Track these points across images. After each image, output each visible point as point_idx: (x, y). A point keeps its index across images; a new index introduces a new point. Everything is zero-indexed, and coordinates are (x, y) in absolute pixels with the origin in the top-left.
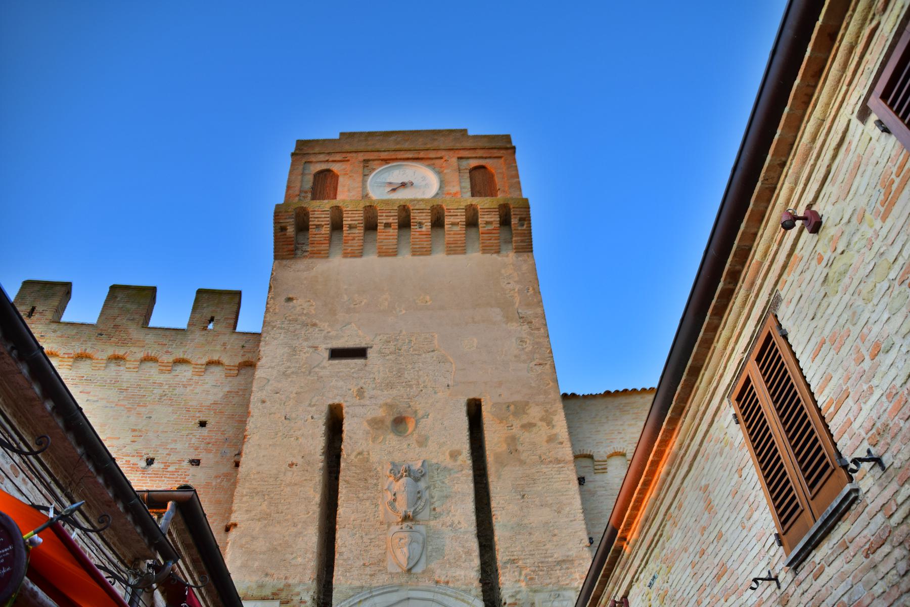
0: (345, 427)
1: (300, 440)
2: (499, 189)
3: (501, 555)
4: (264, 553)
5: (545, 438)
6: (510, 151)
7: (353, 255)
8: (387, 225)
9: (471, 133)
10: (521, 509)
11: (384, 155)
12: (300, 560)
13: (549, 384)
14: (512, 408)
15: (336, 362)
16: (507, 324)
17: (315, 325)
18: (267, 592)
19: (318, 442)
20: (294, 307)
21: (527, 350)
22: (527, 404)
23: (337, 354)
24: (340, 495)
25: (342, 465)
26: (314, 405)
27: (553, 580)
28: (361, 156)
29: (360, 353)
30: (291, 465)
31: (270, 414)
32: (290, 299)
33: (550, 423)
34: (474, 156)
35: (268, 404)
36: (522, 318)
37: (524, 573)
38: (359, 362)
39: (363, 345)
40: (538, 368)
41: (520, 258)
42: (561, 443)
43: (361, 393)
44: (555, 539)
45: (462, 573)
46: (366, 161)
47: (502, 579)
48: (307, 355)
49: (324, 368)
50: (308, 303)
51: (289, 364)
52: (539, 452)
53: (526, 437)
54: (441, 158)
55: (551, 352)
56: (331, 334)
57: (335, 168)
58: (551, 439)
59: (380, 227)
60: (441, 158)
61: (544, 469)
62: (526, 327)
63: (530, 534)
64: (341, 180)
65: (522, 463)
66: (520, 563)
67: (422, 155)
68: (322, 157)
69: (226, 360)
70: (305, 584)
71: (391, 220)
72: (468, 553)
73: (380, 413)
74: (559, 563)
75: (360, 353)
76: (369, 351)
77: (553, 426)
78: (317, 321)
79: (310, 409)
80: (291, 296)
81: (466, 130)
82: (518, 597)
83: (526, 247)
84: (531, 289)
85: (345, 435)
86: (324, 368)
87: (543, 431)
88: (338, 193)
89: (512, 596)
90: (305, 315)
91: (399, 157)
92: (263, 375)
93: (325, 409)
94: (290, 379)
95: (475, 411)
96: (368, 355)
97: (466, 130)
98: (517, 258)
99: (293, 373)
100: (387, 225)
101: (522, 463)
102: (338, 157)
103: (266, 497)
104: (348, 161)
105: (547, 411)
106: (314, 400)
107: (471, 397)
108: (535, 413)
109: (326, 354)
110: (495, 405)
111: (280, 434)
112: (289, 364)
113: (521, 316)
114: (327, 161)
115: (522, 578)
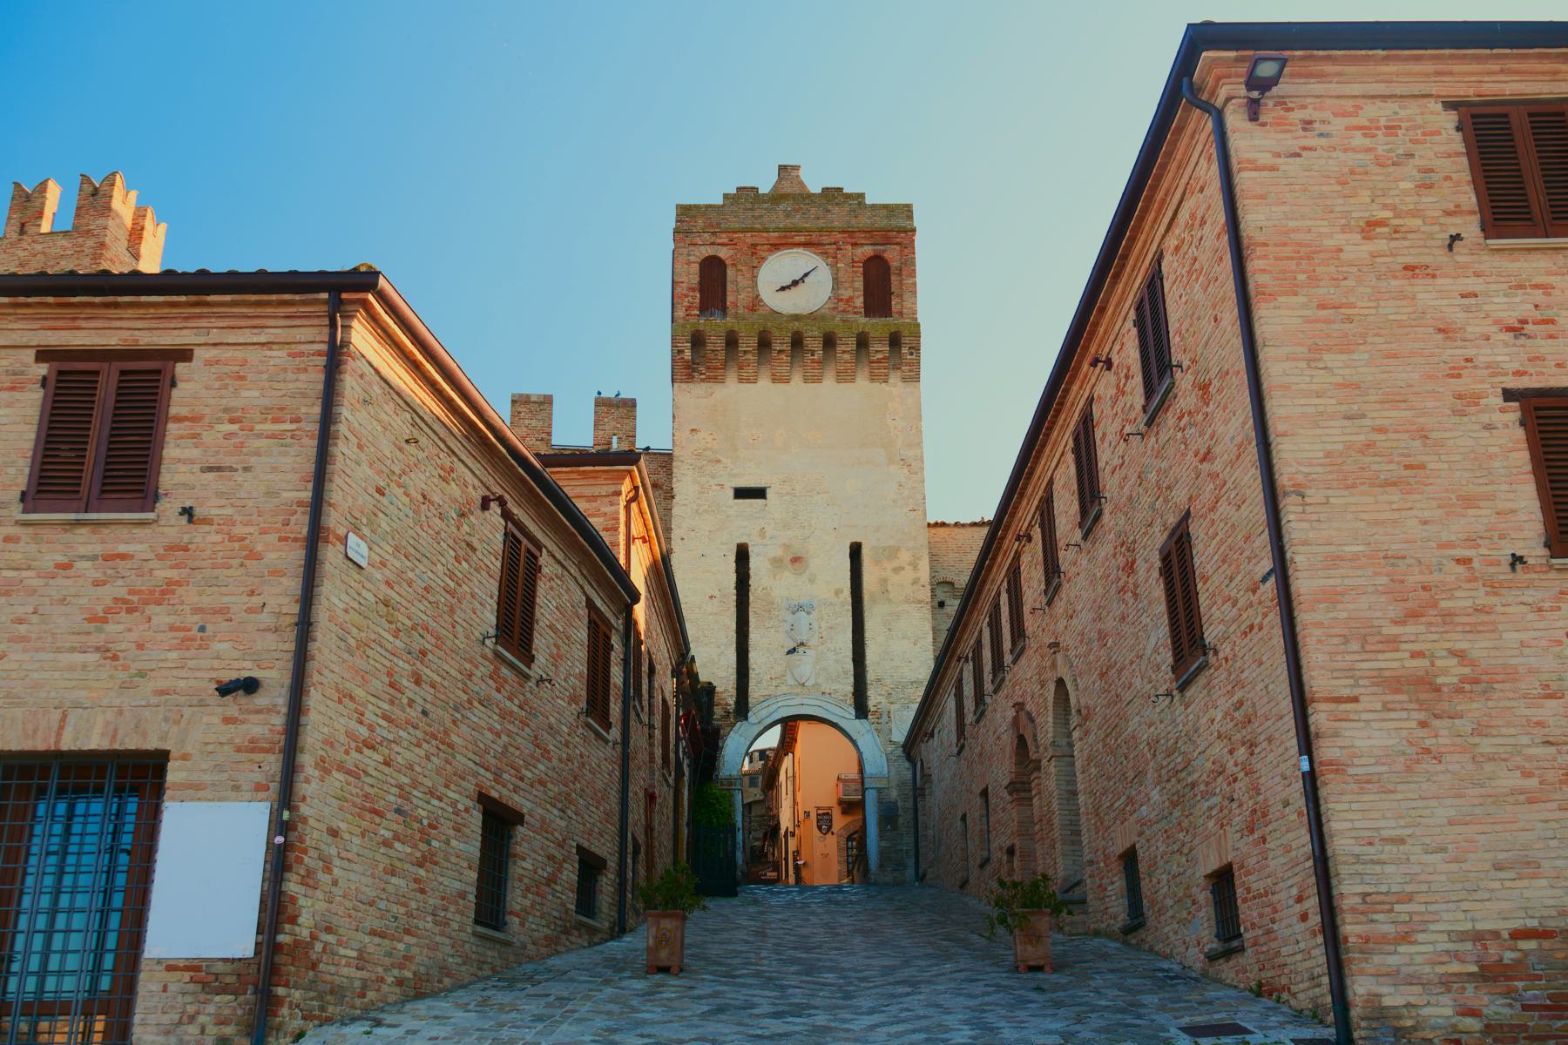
7: (748, 381)
8: (780, 352)
9: (869, 201)
17: (719, 461)
22: (898, 549)
23: (741, 493)
25: (751, 598)
28: (749, 239)
29: (759, 493)
33: (915, 568)
38: (759, 502)
39: (763, 485)
43: (762, 532)
49: (731, 507)
53: (894, 579)
55: (924, 498)
57: (723, 253)
58: (915, 582)
59: (774, 354)
64: (730, 272)
65: (890, 601)
71: (784, 348)
72: (845, 673)
73: (779, 553)
74: (912, 683)
75: (759, 493)
76: (768, 491)
81: (862, 196)
83: (913, 377)
85: (751, 572)
86: (731, 507)
87: (908, 575)
95: (856, 551)
96: (768, 496)
97: (862, 196)
100: (780, 352)
101: (890, 601)
108: (904, 557)
109: (731, 493)
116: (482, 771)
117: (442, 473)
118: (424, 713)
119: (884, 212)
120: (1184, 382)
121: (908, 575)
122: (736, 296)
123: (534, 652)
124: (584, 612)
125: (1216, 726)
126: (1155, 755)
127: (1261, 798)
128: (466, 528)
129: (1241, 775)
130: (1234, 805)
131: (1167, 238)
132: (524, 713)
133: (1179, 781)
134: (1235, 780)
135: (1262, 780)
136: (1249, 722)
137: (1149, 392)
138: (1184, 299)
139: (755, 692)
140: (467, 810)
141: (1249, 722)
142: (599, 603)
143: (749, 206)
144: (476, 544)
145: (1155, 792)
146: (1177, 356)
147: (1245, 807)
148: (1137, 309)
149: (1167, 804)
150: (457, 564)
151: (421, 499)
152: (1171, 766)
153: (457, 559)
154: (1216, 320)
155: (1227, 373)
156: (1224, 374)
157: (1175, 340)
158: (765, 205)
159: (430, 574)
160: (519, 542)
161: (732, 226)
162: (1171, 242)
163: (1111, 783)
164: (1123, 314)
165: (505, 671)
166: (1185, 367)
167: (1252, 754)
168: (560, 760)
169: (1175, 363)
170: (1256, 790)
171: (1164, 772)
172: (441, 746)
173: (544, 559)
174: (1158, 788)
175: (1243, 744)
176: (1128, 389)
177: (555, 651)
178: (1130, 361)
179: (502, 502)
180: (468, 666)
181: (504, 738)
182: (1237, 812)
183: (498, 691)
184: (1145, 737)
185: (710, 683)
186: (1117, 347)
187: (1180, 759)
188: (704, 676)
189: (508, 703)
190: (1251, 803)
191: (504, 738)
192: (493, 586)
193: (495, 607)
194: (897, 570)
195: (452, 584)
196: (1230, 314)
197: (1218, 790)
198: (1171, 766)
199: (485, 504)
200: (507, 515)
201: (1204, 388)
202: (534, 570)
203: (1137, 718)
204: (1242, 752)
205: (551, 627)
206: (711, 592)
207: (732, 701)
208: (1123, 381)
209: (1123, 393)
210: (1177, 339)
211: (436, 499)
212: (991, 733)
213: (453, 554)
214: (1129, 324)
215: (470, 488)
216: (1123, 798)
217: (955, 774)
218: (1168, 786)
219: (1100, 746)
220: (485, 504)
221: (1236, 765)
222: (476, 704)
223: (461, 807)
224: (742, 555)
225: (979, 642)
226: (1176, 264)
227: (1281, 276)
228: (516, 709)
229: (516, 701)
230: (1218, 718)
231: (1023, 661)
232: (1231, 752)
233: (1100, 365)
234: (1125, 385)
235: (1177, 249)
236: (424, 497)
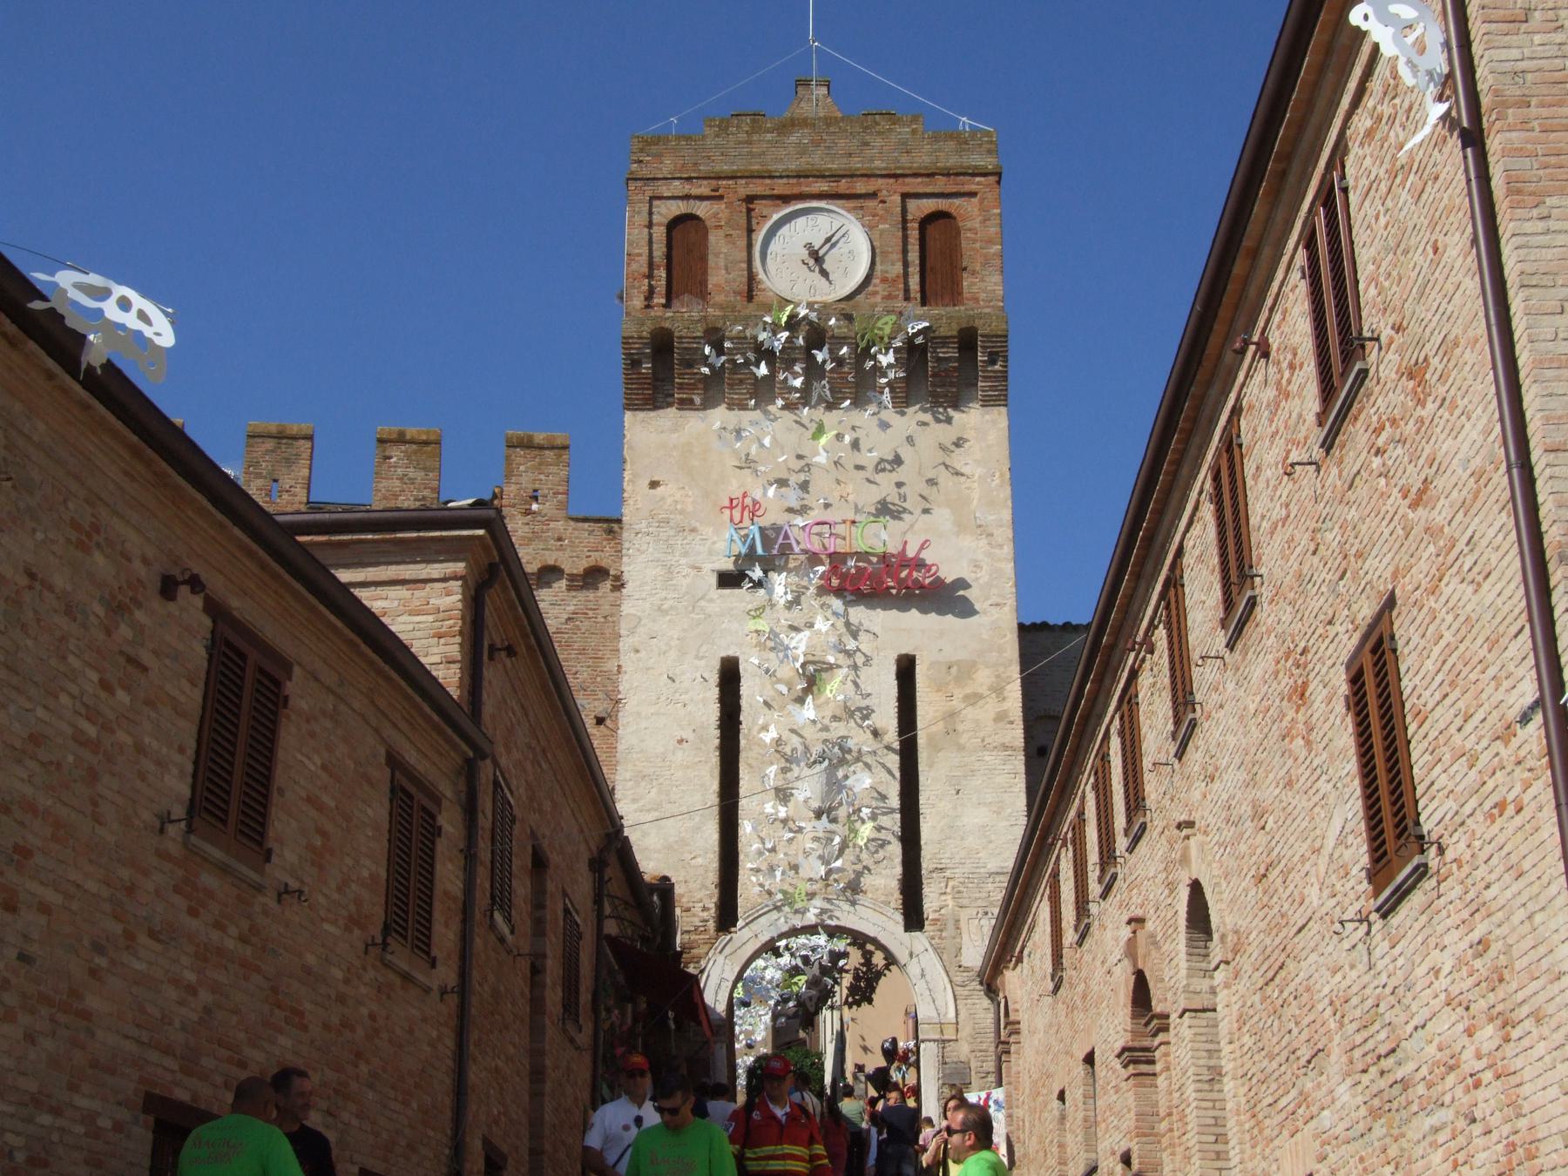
0: (745, 690)
1: (689, 708)
2: (965, 269)
3: (927, 863)
4: (659, 852)
5: (992, 715)
6: (992, 179)
10: (955, 808)
11: (781, 187)
12: (699, 861)
13: (1005, 636)
14: (954, 670)
15: (727, 592)
16: (958, 536)
17: (693, 530)
19: (711, 712)
20: (663, 499)
21: (981, 581)
24: (741, 783)
25: (743, 742)
26: (702, 658)
27: (984, 895)
28: (744, 188)
30: (681, 741)
31: (648, 669)
32: (654, 484)
34: (929, 190)
35: (643, 654)
36: (980, 526)
37: (951, 883)
40: (994, 610)
41: (987, 417)
42: (1012, 723)
44: (991, 846)
45: (883, 881)
46: (750, 199)
47: (926, 890)
48: (689, 580)
49: (711, 600)
50: (682, 492)
51: (664, 594)
52: (981, 734)
53: (970, 713)
54: (873, 195)
56: (717, 545)
57: (702, 209)
60: (873, 195)
61: (988, 757)
62: (983, 542)
63: (962, 839)
65: (961, 748)
66: (948, 873)
67: (843, 186)
68: (677, 187)
69: (567, 567)
77: (1004, 699)
78: (698, 525)
79: (697, 662)
80: (655, 479)
82: (943, 911)
84: (997, 474)
85: (744, 703)
86: (711, 600)
87: (990, 708)
88: (709, 271)
90: (682, 512)
91: (806, 189)
92: (632, 611)
93: (717, 665)
94: (668, 618)
98: (983, 415)
99: (672, 607)
101: (961, 748)
102: (704, 188)
103: (655, 783)
104: (721, 197)
105: (998, 676)
106: (704, 648)
107: (904, 652)
108: (983, 679)
109: (714, 580)
110: (932, 664)
111: (663, 698)
112: (664, 594)
113: (979, 522)
114: (687, 197)
115: (949, 890)
116: (154, 1056)
117: (73, 536)
118: (23, 958)
119: (951, 144)
120: (1384, 364)
121: (990, 708)
122: (722, 275)
123: (271, 844)
124: (382, 774)
125: (1442, 983)
126: (1342, 1025)
127: (1522, 1123)
128: (125, 631)
129: (1488, 1076)
130: (1477, 1129)
131: (1355, 118)
132: (248, 951)
133: (1382, 1073)
134: (1477, 1085)
135: (1526, 1090)
136: (1501, 980)
137: (1327, 390)
138: (1382, 221)
139: (749, 887)
140: (118, 1127)
141: (1501, 980)
142: (411, 757)
143: (743, 137)
144: (146, 657)
145: (1342, 1088)
146: (1372, 320)
147: (1495, 1136)
148: (1307, 247)
149: (1363, 1111)
150: (103, 695)
151: (24, 581)
152: (1370, 1045)
153: (105, 685)
154: (1436, 251)
155: (1456, 345)
156: (1448, 347)
157: (1368, 293)
158: (769, 136)
159: (40, 712)
160: (242, 656)
161: (718, 168)
162: (1361, 122)
163: (1275, 1065)
164: (1285, 259)
165: (208, 880)
166: (1383, 339)
167: (1507, 1040)
168: (327, 1027)
169: (1366, 334)
170: (1513, 1106)
171: (1357, 1053)
172: (62, 1018)
173: (294, 687)
174: (1349, 1081)
175: (1491, 1020)
176: (1293, 388)
177: (318, 842)
178: (1295, 340)
179: (195, 583)
180: (125, 873)
181: (205, 996)
182: (1479, 1142)
183: (193, 912)
184: (1326, 990)
185: (666, 879)
186: (1277, 318)
187: (1383, 1035)
188: (650, 865)
189: (215, 935)
190: (1506, 1129)
191: (205, 996)
192: (187, 732)
193: (190, 768)
194: (974, 699)
195: (92, 731)
196: (1458, 241)
197: (1447, 1099)
198: (1370, 1045)
199: (168, 588)
200: (214, 608)
201: (1415, 372)
202: (273, 700)
203: (1313, 957)
204: (1488, 1035)
205: (311, 800)
206: (679, 734)
207: (711, 904)
208: (1287, 374)
209: (1287, 396)
210: (1372, 291)
211: (60, 581)
212: (1098, 963)
213: (94, 676)
214: (1295, 275)
215: (137, 565)
216: (1294, 1093)
217: (1051, 1025)
218: (1365, 1079)
219: (1257, 998)
220: (168, 588)
221: (1479, 1057)
222: (143, 939)
223: (105, 1123)
224: (730, 676)
225: (1081, 813)
226: (1368, 161)
227: (1553, 160)
228: (230, 944)
229: (233, 931)
230: (1446, 969)
231: (1142, 847)
232: (1470, 1032)
233: (1252, 348)
234: (1289, 382)
235: (1369, 134)
236: (32, 576)
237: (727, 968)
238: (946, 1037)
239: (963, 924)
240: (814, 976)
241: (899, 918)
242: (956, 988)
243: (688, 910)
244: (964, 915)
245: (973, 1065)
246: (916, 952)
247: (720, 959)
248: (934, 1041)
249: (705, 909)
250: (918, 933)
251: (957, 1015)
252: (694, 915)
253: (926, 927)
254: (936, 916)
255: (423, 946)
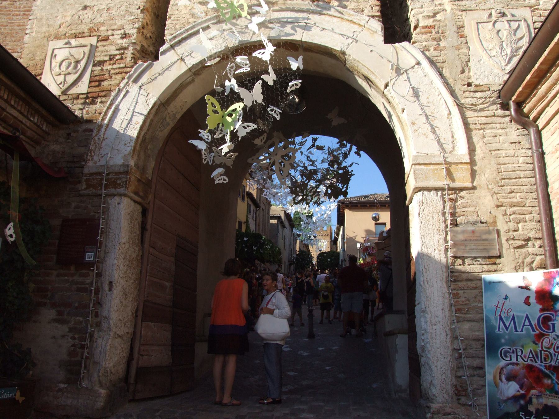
18: (84, 28)
70: (131, 14)
82: (438, 17)
89: (429, 17)
237: (142, 99)
238: (458, 184)
239: (470, 31)
240: (255, 105)
241: (377, 26)
242: (469, 114)
243: (106, 39)
244: (469, 21)
245: (502, 226)
246: (403, 65)
247: (134, 89)
248: (437, 189)
249: (125, 36)
250: (405, 44)
251: (472, 150)
252: (111, 45)
253: (415, 35)
254: (430, 22)
255: (239, 222)
